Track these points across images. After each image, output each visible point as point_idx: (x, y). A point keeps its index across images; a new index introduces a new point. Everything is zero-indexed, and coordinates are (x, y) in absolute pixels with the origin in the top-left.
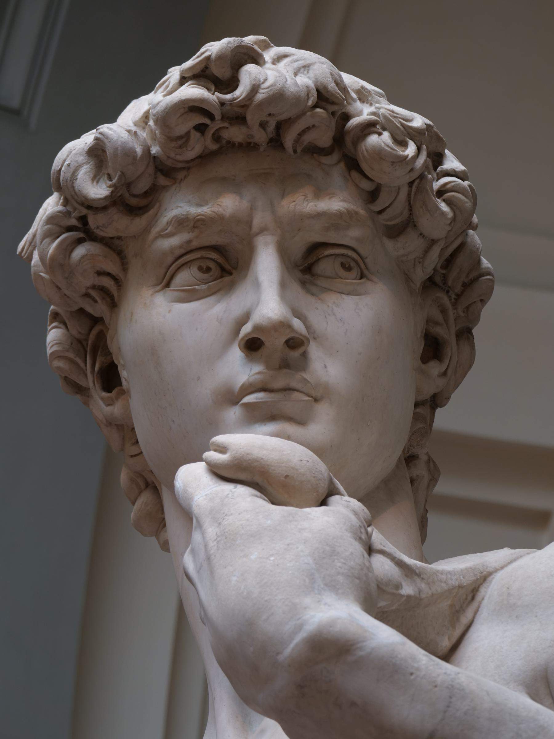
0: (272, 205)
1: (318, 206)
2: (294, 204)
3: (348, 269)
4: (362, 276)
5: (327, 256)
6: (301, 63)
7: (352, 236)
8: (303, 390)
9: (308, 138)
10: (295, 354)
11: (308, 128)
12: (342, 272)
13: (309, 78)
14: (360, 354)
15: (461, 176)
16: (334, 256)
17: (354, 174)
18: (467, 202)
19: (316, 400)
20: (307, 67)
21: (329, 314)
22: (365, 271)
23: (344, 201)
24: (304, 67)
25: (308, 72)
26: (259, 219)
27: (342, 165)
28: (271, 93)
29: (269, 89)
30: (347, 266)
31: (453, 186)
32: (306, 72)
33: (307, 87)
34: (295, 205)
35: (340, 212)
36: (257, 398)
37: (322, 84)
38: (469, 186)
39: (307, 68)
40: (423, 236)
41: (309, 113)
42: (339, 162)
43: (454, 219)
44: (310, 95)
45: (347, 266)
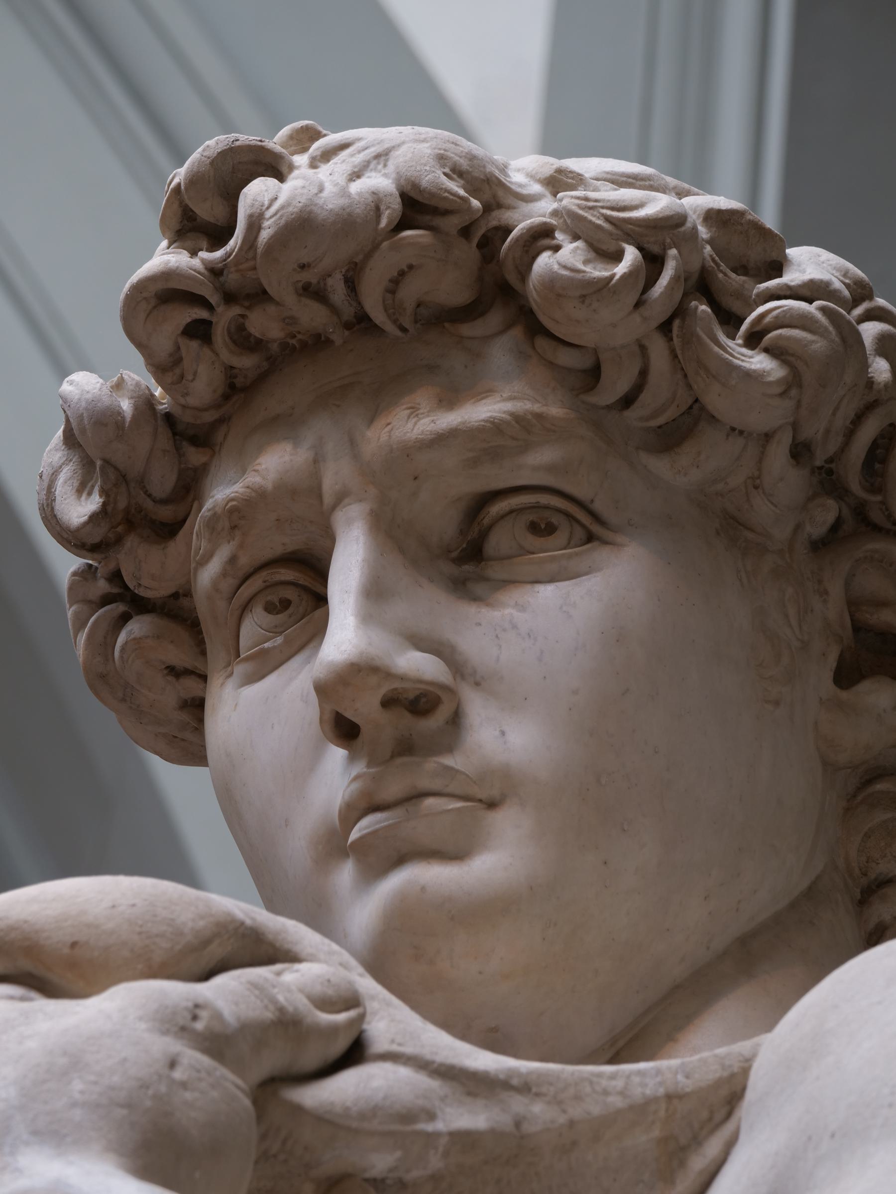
0: (352, 443)
1: (438, 423)
2: (387, 429)
3: (550, 530)
4: (590, 538)
5: (503, 517)
6: (373, 151)
7: (537, 463)
8: (450, 789)
9: (410, 292)
10: (435, 722)
11: (402, 274)
12: (531, 541)
13: (386, 175)
14: (575, 692)
15: (806, 293)
16: (514, 514)
17: (541, 343)
18: (813, 341)
19: (492, 805)
20: (382, 156)
21: (504, 630)
22: (596, 528)
23: (511, 398)
24: (378, 157)
25: (385, 166)
26: (336, 474)
27: (517, 332)
28: (283, 222)
29: (278, 215)
30: (543, 526)
31: (777, 317)
32: (380, 167)
33: (373, 193)
34: (390, 432)
35: (493, 423)
36: (360, 830)
37: (408, 180)
38: (823, 309)
39: (383, 158)
40: (741, 433)
41: (385, 244)
42: (508, 327)
43: (794, 382)
44: (382, 207)
45: (543, 526)
